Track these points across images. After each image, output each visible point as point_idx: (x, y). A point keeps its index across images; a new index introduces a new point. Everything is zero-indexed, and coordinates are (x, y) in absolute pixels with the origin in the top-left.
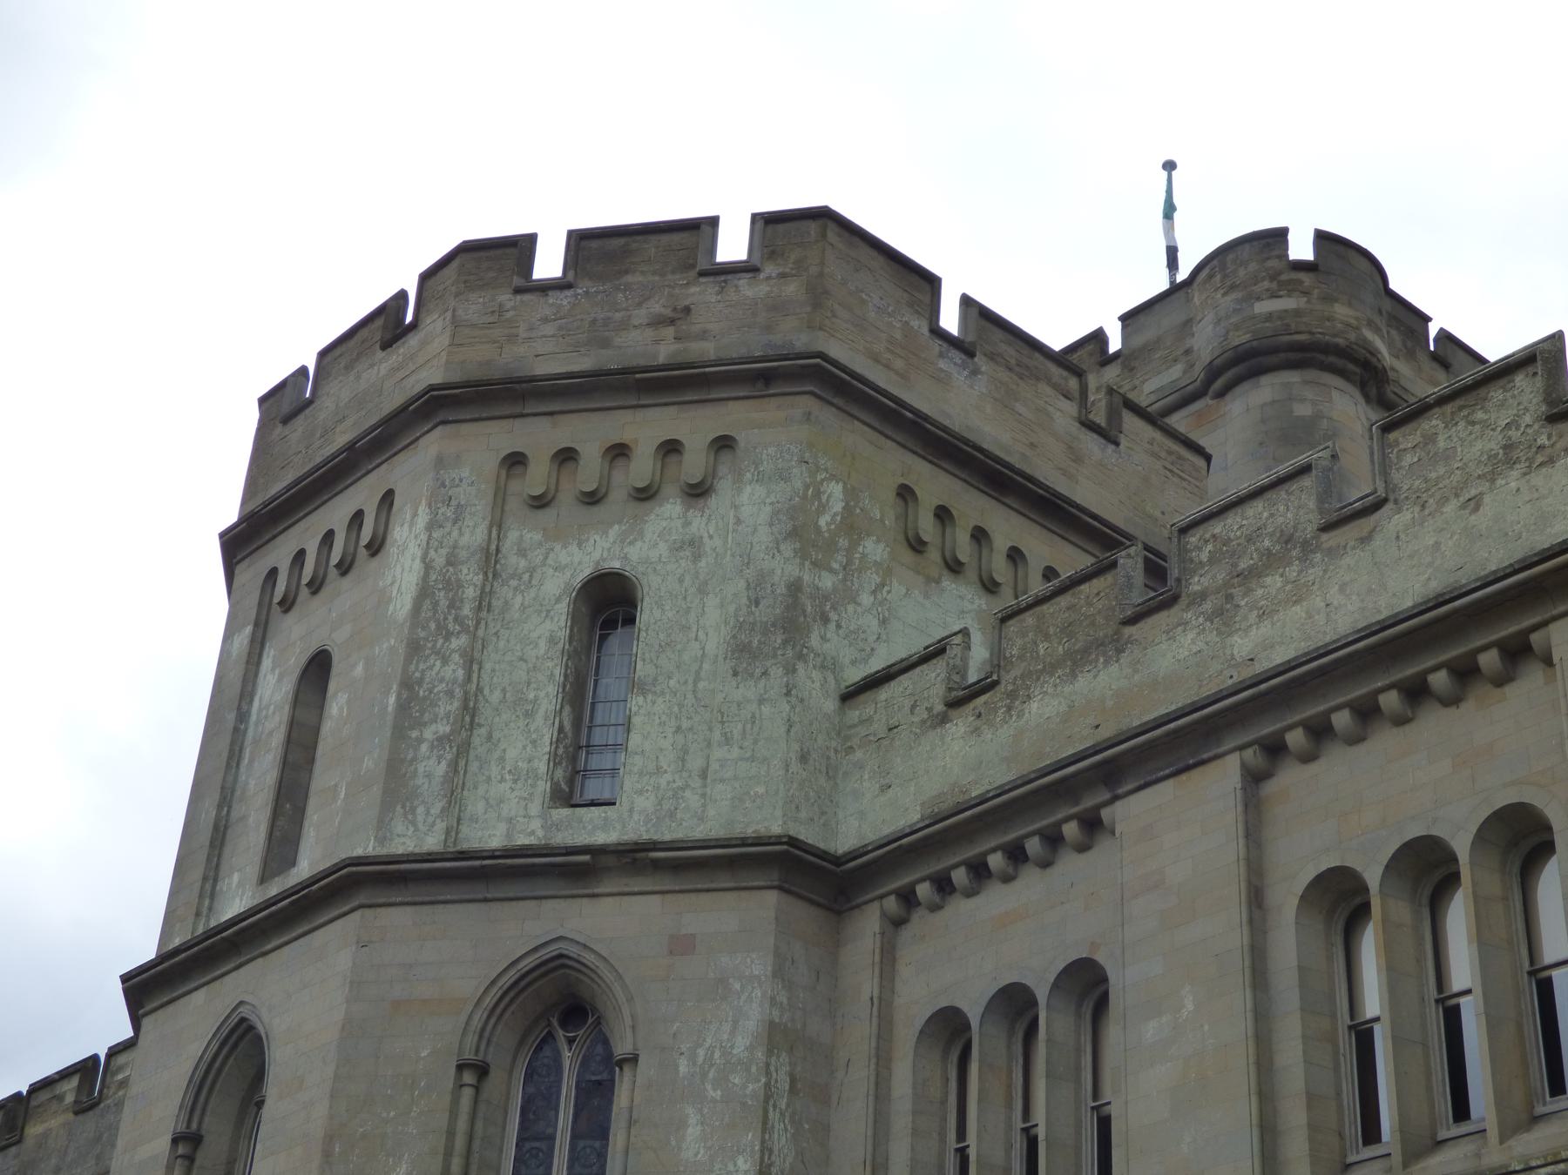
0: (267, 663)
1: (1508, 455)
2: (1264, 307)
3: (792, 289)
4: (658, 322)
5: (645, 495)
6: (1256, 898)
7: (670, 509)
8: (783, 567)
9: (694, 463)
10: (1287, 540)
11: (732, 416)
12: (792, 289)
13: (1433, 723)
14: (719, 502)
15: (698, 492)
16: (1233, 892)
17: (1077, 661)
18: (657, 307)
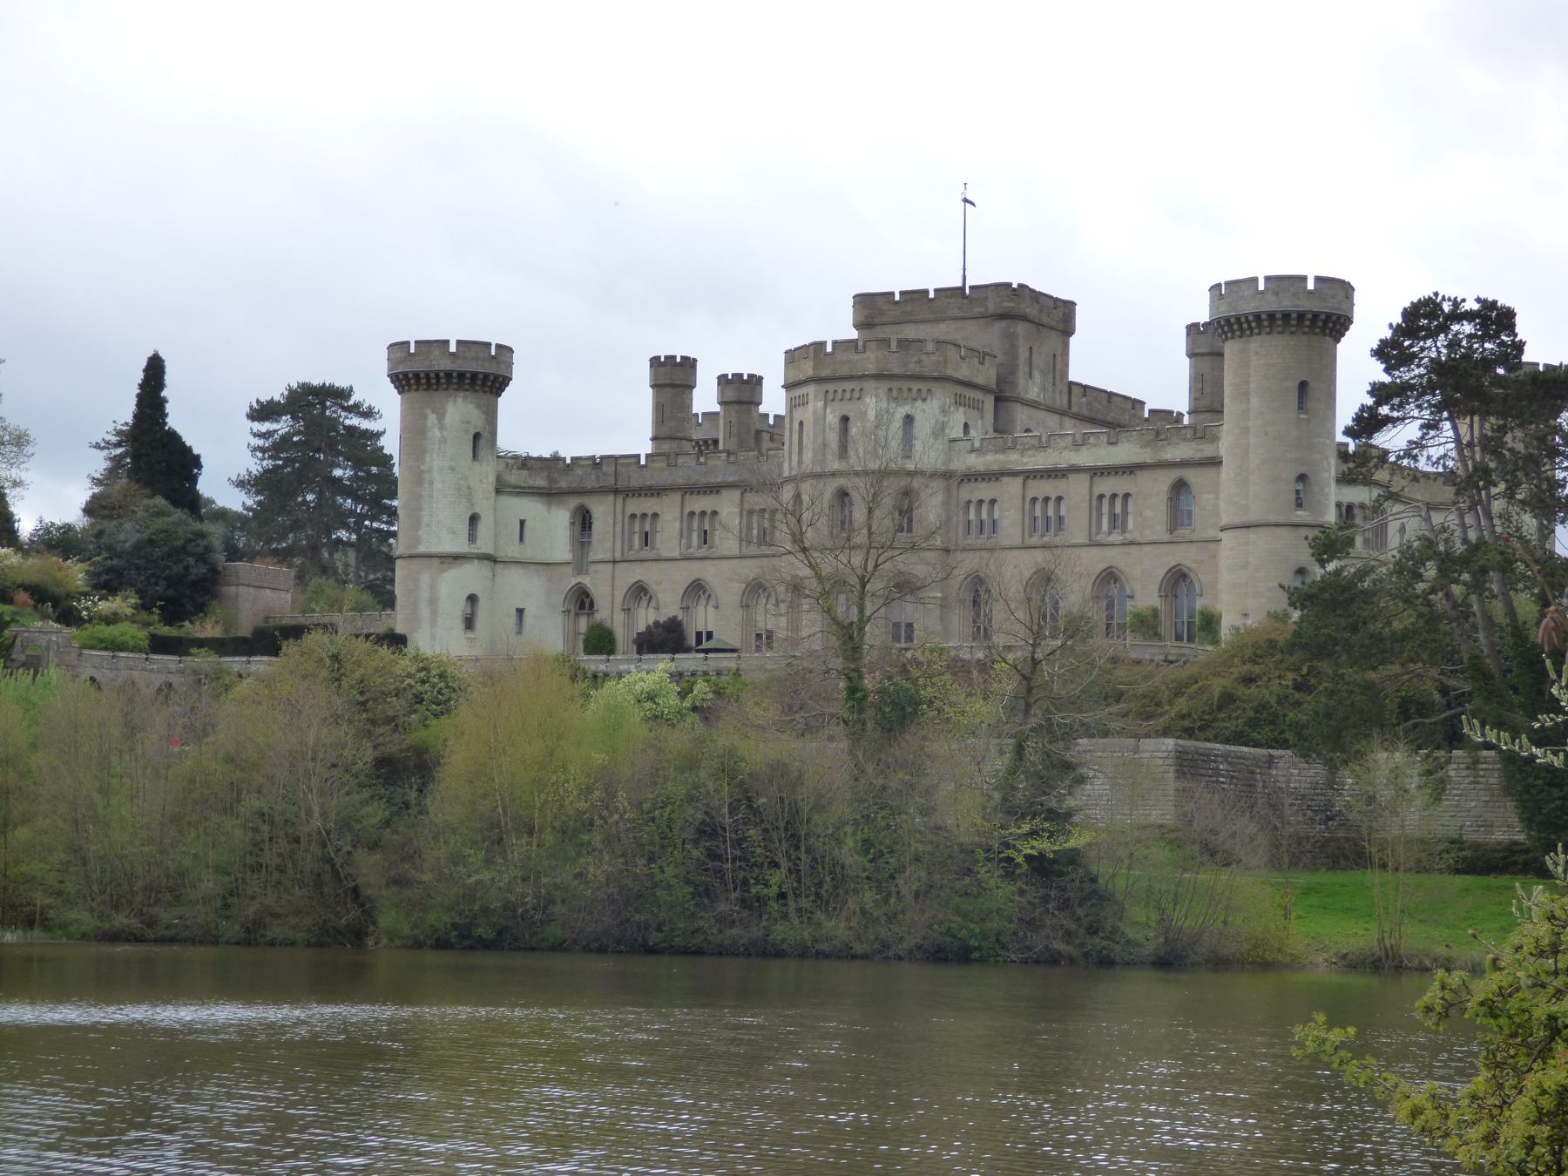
0: (828, 411)
1: (1065, 448)
2: (1006, 304)
3: (941, 359)
4: (916, 363)
5: (915, 400)
6: (1024, 499)
7: (920, 402)
8: (941, 418)
9: (924, 394)
10: (1033, 446)
11: (931, 385)
12: (941, 359)
13: (1050, 481)
14: (928, 401)
15: (924, 400)
16: (1021, 497)
17: (997, 452)
18: (915, 359)
